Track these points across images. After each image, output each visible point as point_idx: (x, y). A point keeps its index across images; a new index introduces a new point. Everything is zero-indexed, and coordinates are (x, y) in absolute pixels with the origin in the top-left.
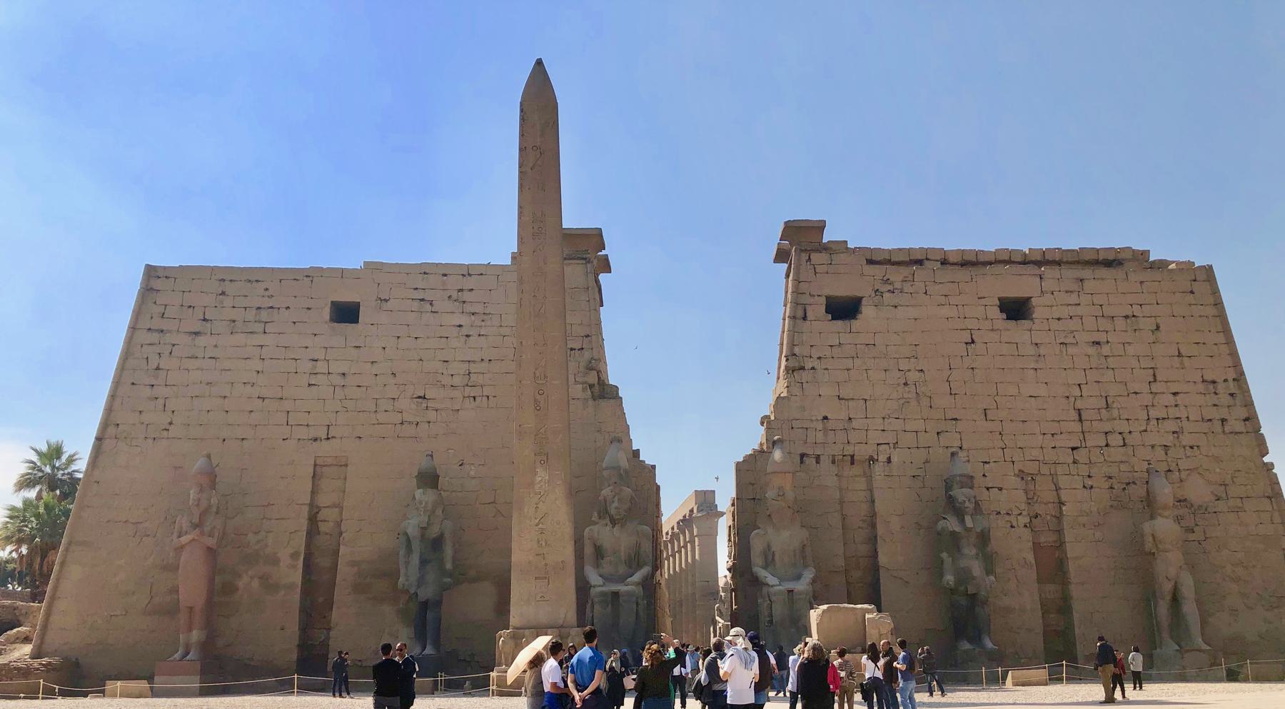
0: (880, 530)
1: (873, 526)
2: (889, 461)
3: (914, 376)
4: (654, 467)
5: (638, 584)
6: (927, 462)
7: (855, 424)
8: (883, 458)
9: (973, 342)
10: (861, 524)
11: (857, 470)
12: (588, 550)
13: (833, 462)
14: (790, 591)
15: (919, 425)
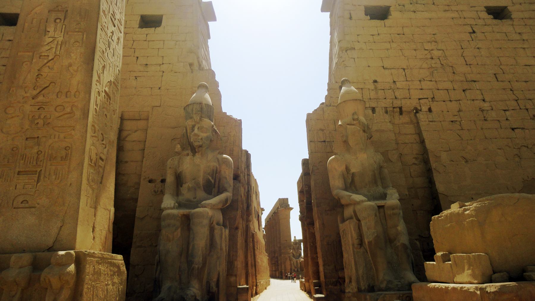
0: (433, 165)
1: (426, 161)
2: (430, 110)
3: (436, 53)
4: (240, 120)
5: (213, 207)
6: (460, 111)
7: (398, 85)
8: (425, 109)
9: (474, 32)
10: (414, 161)
11: (405, 118)
12: (170, 179)
13: (386, 112)
14: (380, 207)
15: (448, 85)
